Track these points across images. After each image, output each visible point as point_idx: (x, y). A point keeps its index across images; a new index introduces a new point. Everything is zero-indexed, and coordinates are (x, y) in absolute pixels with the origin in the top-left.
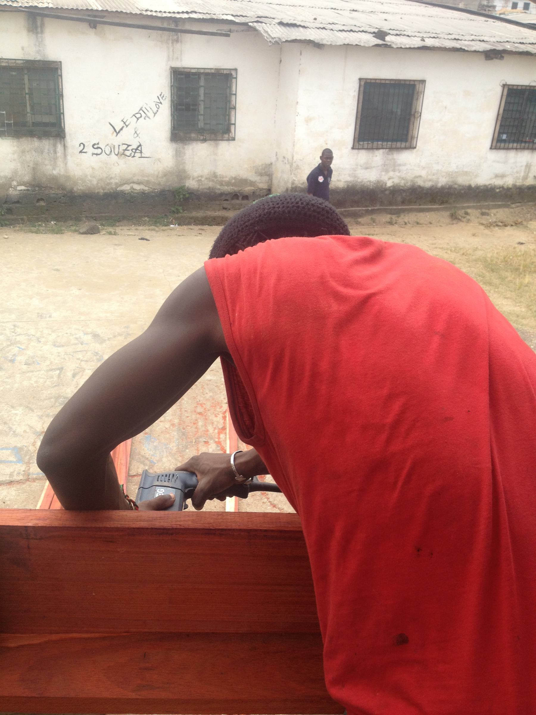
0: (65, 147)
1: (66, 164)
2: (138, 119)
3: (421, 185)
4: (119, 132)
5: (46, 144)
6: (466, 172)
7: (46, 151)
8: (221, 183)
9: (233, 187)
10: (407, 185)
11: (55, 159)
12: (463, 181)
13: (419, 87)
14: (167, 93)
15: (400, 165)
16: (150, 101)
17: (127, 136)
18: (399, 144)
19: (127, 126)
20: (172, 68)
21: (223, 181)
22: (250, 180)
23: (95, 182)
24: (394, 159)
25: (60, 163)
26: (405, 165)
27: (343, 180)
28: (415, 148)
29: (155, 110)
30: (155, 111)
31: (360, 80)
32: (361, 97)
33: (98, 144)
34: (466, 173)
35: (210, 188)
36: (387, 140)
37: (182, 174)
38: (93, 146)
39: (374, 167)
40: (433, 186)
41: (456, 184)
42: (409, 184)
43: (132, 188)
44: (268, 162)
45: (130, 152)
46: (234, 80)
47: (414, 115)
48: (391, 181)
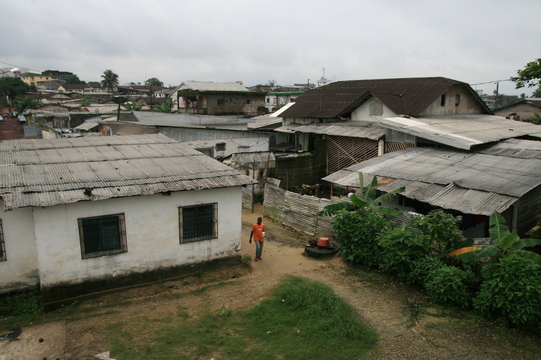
3: (137, 272)
6: (167, 259)
10: (127, 273)
12: (165, 265)
13: (121, 217)
15: (119, 263)
18: (115, 251)
24: (114, 260)
26: (122, 262)
27: (80, 278)
28: (127, 252)
31: (78, 219)
32: (82, 229)
34: (167, 260)
36: (106, 250)
39: (101, 267)
40: (146, 271)
41: (162, 267)
42: (129, 272)
44: (35, 269)
47: (121, 233)
48: (115, 273)
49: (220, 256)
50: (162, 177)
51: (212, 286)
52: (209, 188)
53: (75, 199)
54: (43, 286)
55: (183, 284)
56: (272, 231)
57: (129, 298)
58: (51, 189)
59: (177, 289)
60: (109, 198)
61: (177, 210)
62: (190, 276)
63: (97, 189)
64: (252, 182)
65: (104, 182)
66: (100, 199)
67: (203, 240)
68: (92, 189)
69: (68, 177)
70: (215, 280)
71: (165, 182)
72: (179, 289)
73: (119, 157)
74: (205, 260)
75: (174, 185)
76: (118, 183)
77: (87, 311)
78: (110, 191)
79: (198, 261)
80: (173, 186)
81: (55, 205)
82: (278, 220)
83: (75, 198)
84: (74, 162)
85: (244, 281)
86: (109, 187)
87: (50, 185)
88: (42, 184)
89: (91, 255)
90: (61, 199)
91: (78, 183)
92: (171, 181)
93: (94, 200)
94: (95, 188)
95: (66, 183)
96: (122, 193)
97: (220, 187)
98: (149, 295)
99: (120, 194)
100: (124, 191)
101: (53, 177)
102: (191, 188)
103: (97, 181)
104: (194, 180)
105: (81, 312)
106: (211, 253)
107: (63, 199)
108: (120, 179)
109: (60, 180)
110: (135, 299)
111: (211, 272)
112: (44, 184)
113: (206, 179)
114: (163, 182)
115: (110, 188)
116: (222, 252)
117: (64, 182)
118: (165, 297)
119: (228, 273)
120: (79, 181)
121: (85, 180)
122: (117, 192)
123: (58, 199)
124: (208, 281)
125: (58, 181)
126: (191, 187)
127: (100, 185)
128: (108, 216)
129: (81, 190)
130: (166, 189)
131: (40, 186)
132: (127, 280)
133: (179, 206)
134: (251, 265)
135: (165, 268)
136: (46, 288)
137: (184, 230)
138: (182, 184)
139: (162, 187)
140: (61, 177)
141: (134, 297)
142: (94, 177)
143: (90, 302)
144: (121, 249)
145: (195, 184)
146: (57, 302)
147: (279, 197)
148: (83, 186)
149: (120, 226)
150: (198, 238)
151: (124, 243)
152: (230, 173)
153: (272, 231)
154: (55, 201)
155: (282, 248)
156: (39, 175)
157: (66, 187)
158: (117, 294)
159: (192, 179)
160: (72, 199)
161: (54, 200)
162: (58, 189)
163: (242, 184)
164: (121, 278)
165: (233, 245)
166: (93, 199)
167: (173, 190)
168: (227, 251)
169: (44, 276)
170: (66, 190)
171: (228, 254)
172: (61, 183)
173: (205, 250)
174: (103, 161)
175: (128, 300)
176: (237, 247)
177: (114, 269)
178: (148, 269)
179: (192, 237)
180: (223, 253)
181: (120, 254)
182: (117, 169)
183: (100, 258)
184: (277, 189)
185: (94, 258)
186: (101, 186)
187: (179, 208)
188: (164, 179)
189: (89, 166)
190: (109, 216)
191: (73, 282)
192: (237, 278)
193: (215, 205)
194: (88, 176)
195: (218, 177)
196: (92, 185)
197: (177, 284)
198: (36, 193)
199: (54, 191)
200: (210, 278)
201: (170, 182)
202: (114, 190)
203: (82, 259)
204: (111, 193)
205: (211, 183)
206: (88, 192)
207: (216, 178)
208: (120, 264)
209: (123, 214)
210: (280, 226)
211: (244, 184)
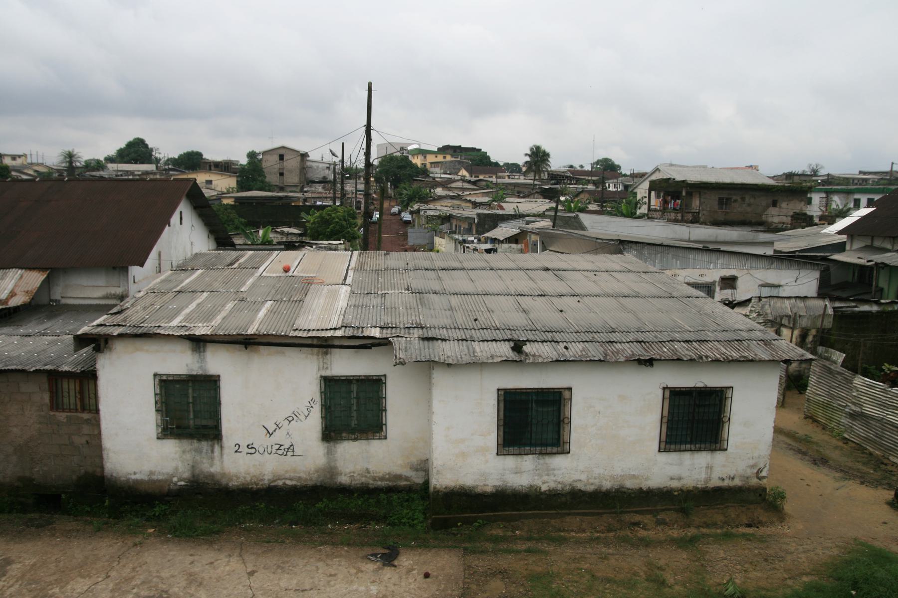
0: (222, 447)
1: (222, 462)
2: (290, 422)
4: (272, 433)
5: (205, 445)
6: (634, 475)
7: (204, 451)
8: (374, 479)
9: (388, 482)
10: (565, 489)
11: (212, 459)
12: (629, 484)
13: (566, 394)
14: (318, 398)
15: (554, 469)
16: (302, 406)
17: (279, 437)
18: (549, 449)
19: (280, 428)
20: (321, 377)
21: (376, 477)
22: (405, 476)
23: (248, 479)
24: (547, 464)
25: (217, 462)
26: (559, 469)
30: (306, 414)
31: (498, 390)
32: (502, 405)
33: (252, 444)
34: (634, 476)
35: (362, 483)
36: (536, 445)
37: (332, 471)
38: (248, 446)
40: (596, 490)
41: (623, 488)
42: (567, 488)
43: (284, 484)
44: (424, 458)
45: (283, 451)
46: (384, 385)
47: (563, 421)
49: (726, 483)
50: (637, 332)
51: (709, 536)
52: (722, 359)
53: (497, 356)
54: (435, 488)
55: (656, 522)
56: (821, 446)
57: (563, 531)
58: (461, 336)
59: (645, 529)
60: (551, 360)
61: (660, 392)
62: (669, 510)
63: (532, 343)
64: (803, 356)
65: (542, 333)
66: (537, 361)
67: (700, 450)
68: (524, 342)
69: (486, 319)
70: (715, 525)
71: (642, 341)
72: (649, 530)
73: (564, 292)
74: (699, 486)
75: (660, 348)
76: (566, 337)
77: (496, 540)
78: (552, 350)
79: (687, 486)
80: (656, 349)
81: (466, 364)
82: (833, 428)
83: (498, 354)
84: (495, 295)
85: (769, 536)
86: (550, 342)
87: (459, 329)
88: (448, 327)
89: (511, 449)
90: (476, 354)
91: (502, 331)
92: (653, 341)
93: (528, 361)
94: (528, 341)
95: (483, 329)
96: (571, 354)
97: (741, 359)
98: (598, 532)
99: (569, 355)
100: (576, 350)
101: (464, 317)
102: (689, 358)
103: (531, 330)
104: (694, 343)
105: (487, 540)
106: (713, 476)
107: (479, 354)
108: (567, 330)
109: (474, 322)
110: (573, 534)
111: (708, 509)
112: (450, 326)
113: (716, 343)
114: (640, 342)
115: (553, 343)
116: (732, 476)
117: (479, 326)
118: (625, 540)
119: (738, 516)
120: (504, 327)
121: (512, 327)
122: (564, 352)
123: (472, 355)
124: (702, 524)
125: (471, 324)
126: (690, 356)
127: (536, 336)
128: (545, 391)
129: (506, 343)
130: (645, 353)
131: (444, 329)
132: (563, 499)
133: (665, 386)
134: (783, 509)
135: (629, 489)
136: (438, 491)
137: (668, 428)
138: (672, 348)
139: (638, 351)
140: (475, 318)
141: (572, 531)
142: (526, 323)
143: (502, 526)
144: (560, 446)
145: (696, 349)
146: (451, 516)
147: (840, 385)
148: (510, 337)
149: (562, 408)
150: (692, 446)
151: (566, 438)
152: (758, 334)
153: (821, 446)
154: (468, 357)
155: (842, 484)
156: (443, 311)
157: (483, 335)
158: (545, 520)
159: (690, 341)
160: (492, 357)
161: (466, 355)
162: (471, 337)
163: (784, 359)
164: (555, 495)
165: (753, 466)
166: (526, 359)
167: (658, 357)
168: (741, 476)
169: (438, 472)
170: (483, 341)
171: (742, 481)
172: (476, 328)
173: (701, 468)
174: (538, 295)
175: (562, 534)
176: (760, 471)
177: (545, 478)
178: (601, 486)
179: (681, 443)
180: (733, 478)
181: (557, 455)
182: (561, 311)
183: (526, 457)
184: (838, 370)
185: (515, 456)
186: (538, 340)
187: (664, 389)
188: (641, 337)
189: (517, 304)
190: (547, 391)
191: (479, 490)
192: (756, 529)
193: (728, 391)
194: (517, 319)
195: (737, 341)
196: (523, 335)
197: (646, 521)
198: (440, 341)
199: (467, 341)
200: (705, 520)
201: (652, 343)
202: (559, 347)
203: (497, 454)
204: (555, 353)
205: (725, 351)
206: (518, 347)
207: (733, 343)
208: (556, 472)
209: (570, 389)
210: (838, 440)
211: (788, 358)
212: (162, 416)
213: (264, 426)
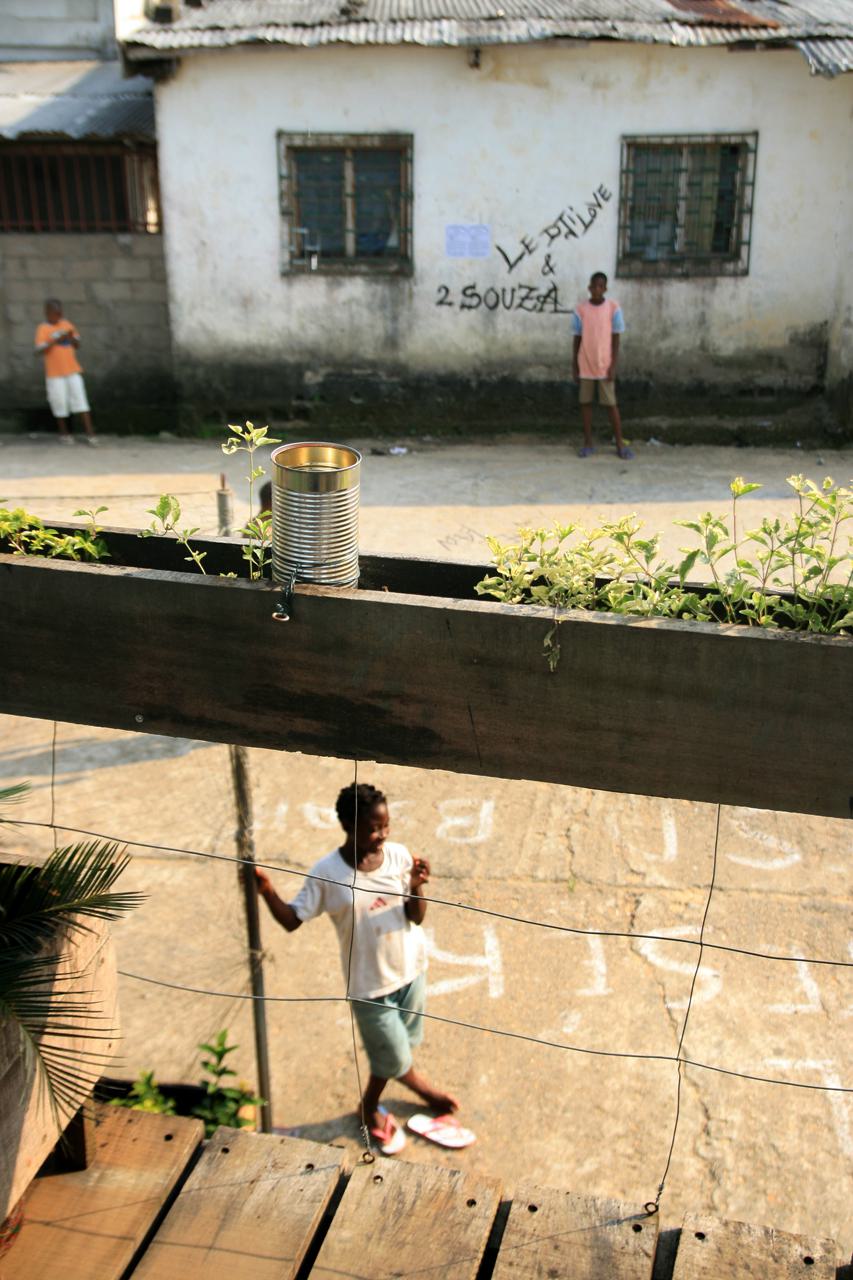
2: (553, 237)
14: (613, 187)
17: (529, 270)
29: (587, 219)
38: (464, 292)
46: (751, 157)
212: (291, 225)
213: (499, 249)
